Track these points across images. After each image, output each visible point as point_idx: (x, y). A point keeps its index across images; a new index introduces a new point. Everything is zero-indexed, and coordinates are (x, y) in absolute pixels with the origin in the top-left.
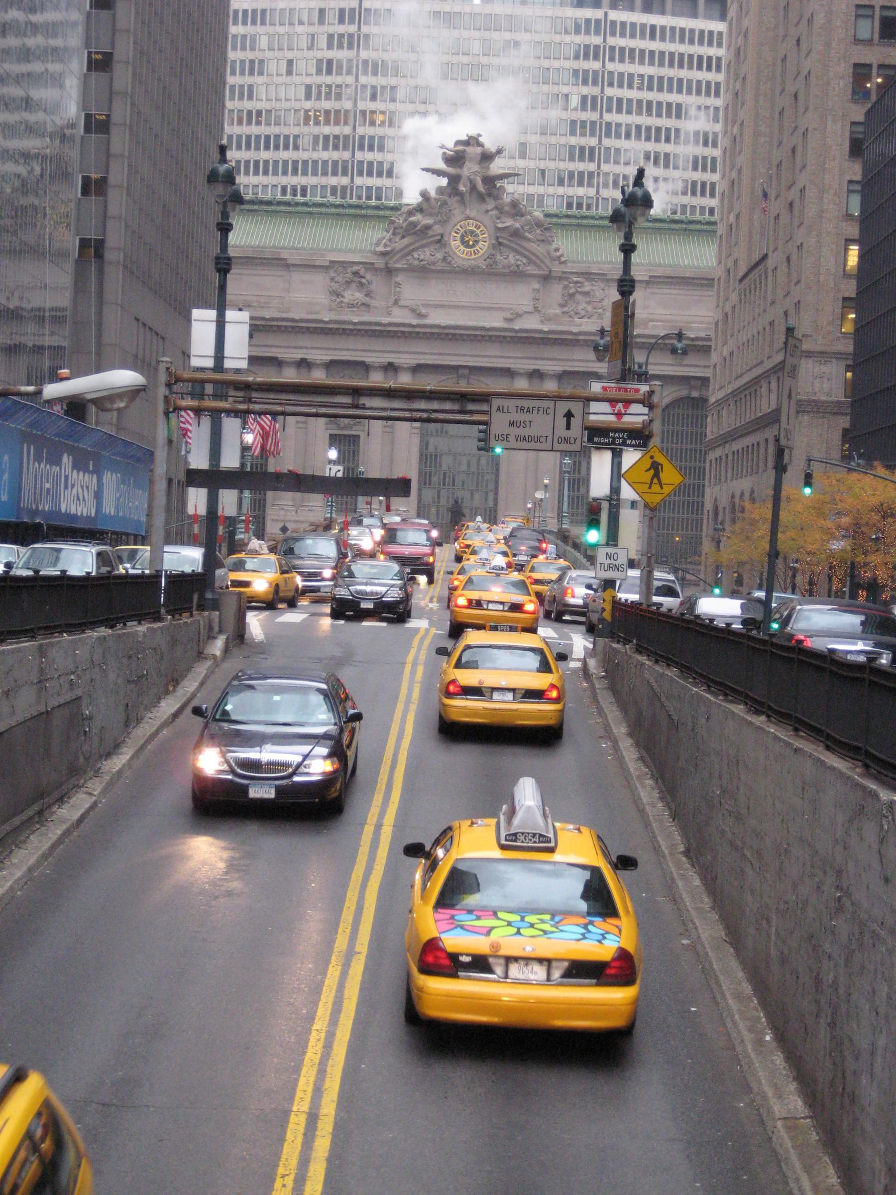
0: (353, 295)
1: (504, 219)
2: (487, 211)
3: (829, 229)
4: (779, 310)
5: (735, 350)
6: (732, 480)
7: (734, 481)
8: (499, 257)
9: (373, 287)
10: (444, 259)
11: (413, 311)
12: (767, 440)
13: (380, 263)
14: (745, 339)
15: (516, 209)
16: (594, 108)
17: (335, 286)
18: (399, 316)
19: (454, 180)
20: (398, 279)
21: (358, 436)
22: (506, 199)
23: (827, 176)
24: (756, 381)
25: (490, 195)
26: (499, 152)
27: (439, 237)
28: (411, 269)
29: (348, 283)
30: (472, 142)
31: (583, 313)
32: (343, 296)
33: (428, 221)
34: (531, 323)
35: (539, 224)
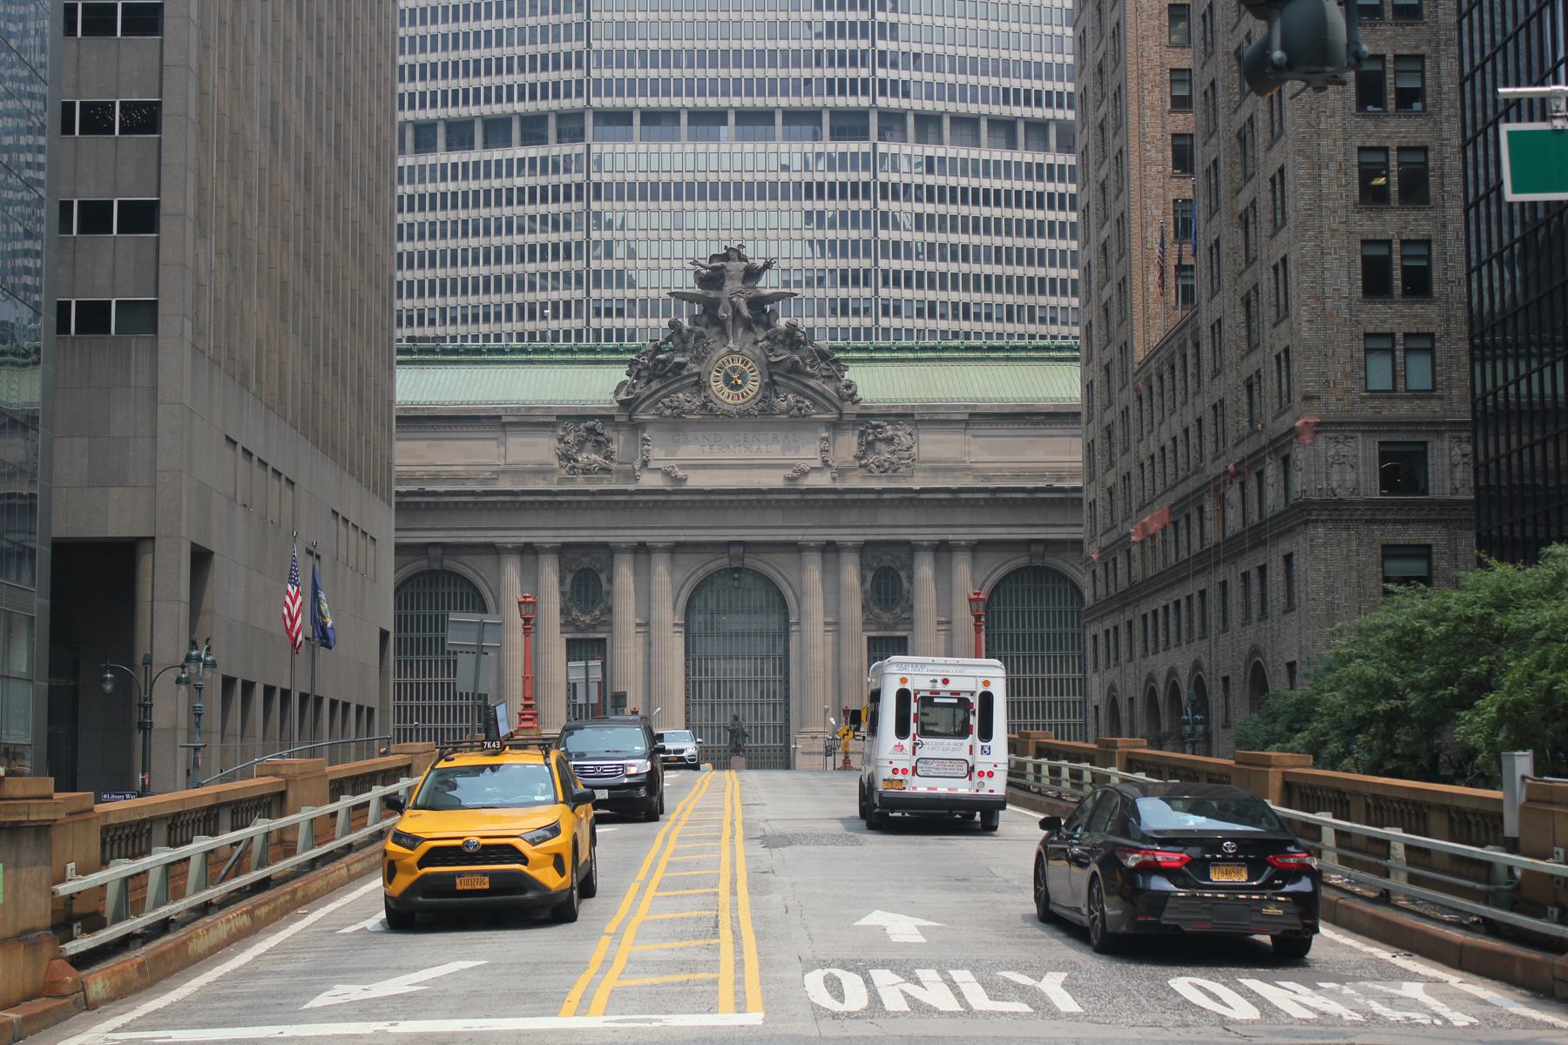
2: (756, 342)
3: (1334, 226)
4: (1229, 386)
5: (1135, 471)
6: (1156, 652)
7: (1161, 654)
9: (613, 447)
10: (704, 406)
11: (667, 474)
12: (1224, 584)
14: (1156, 450)
15: (792, 338)
16: (867, 255)
18: (650, 481)
19: (711, 307)
21: (604, 640)
22: (782, 322)
23: (1323, 142)
24: (1196, 496)
25: (757, 322)
26: (768, 266)
28: (661, 422)
29: (581, 444)
30: (733, 255)
32: (576, 461)
33: (678, 359)
34: (822, 480)
35: (823, 355)
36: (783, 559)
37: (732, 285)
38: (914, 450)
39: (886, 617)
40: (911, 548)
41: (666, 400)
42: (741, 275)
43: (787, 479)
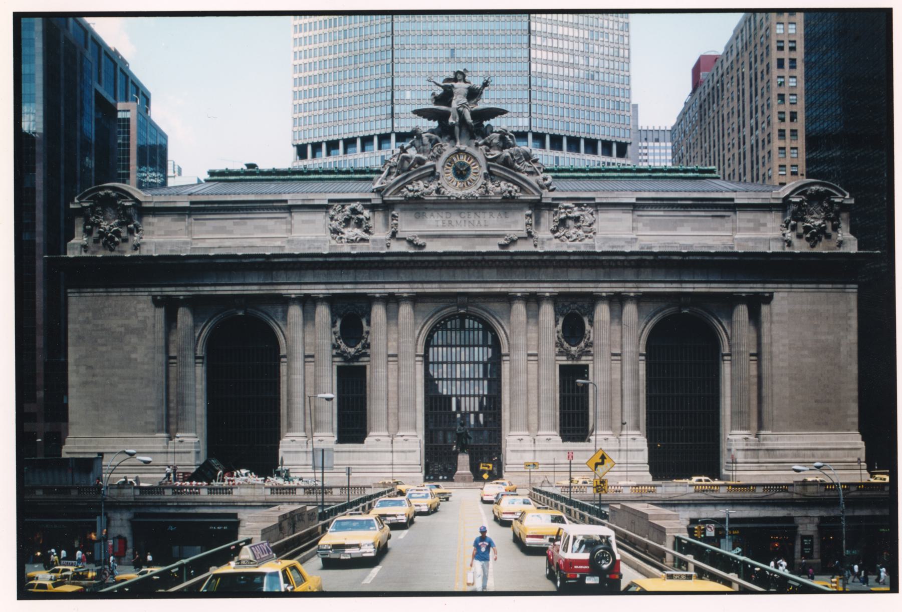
0: (352, 232)
1: (492, 152)
2: (477, 145)
8: (490, 185)
10: (438, 191)
11: (410, 242)
13: (376, 199)
17: (335, 224)
18: (398, 247)
20: (394, 212)
26: (485, 84)
27: (432, 169)
29: (347, 222)
30: (460, 77)
31: (575, 237)
32: (342, 233)
36: (496, 306)
37: (458, 100)
38: (594, 227)
39: (573, 349)
40: (593, 299)
41: (410, 187)
42: (466, 91)
43: (501, 246)
